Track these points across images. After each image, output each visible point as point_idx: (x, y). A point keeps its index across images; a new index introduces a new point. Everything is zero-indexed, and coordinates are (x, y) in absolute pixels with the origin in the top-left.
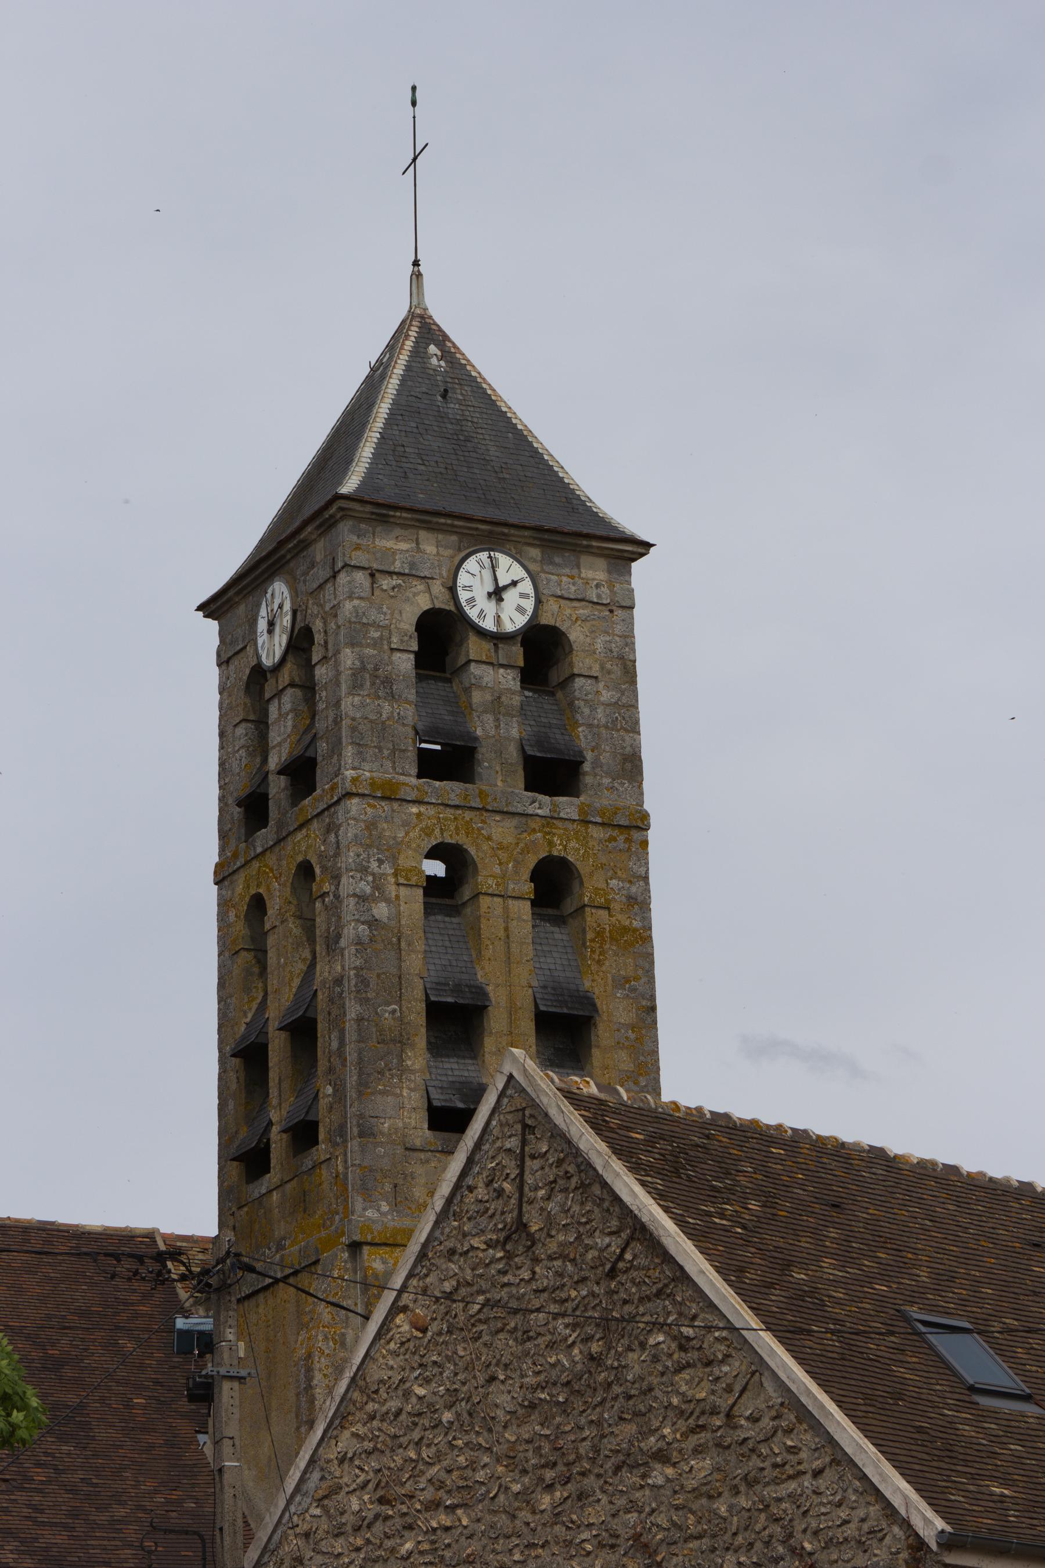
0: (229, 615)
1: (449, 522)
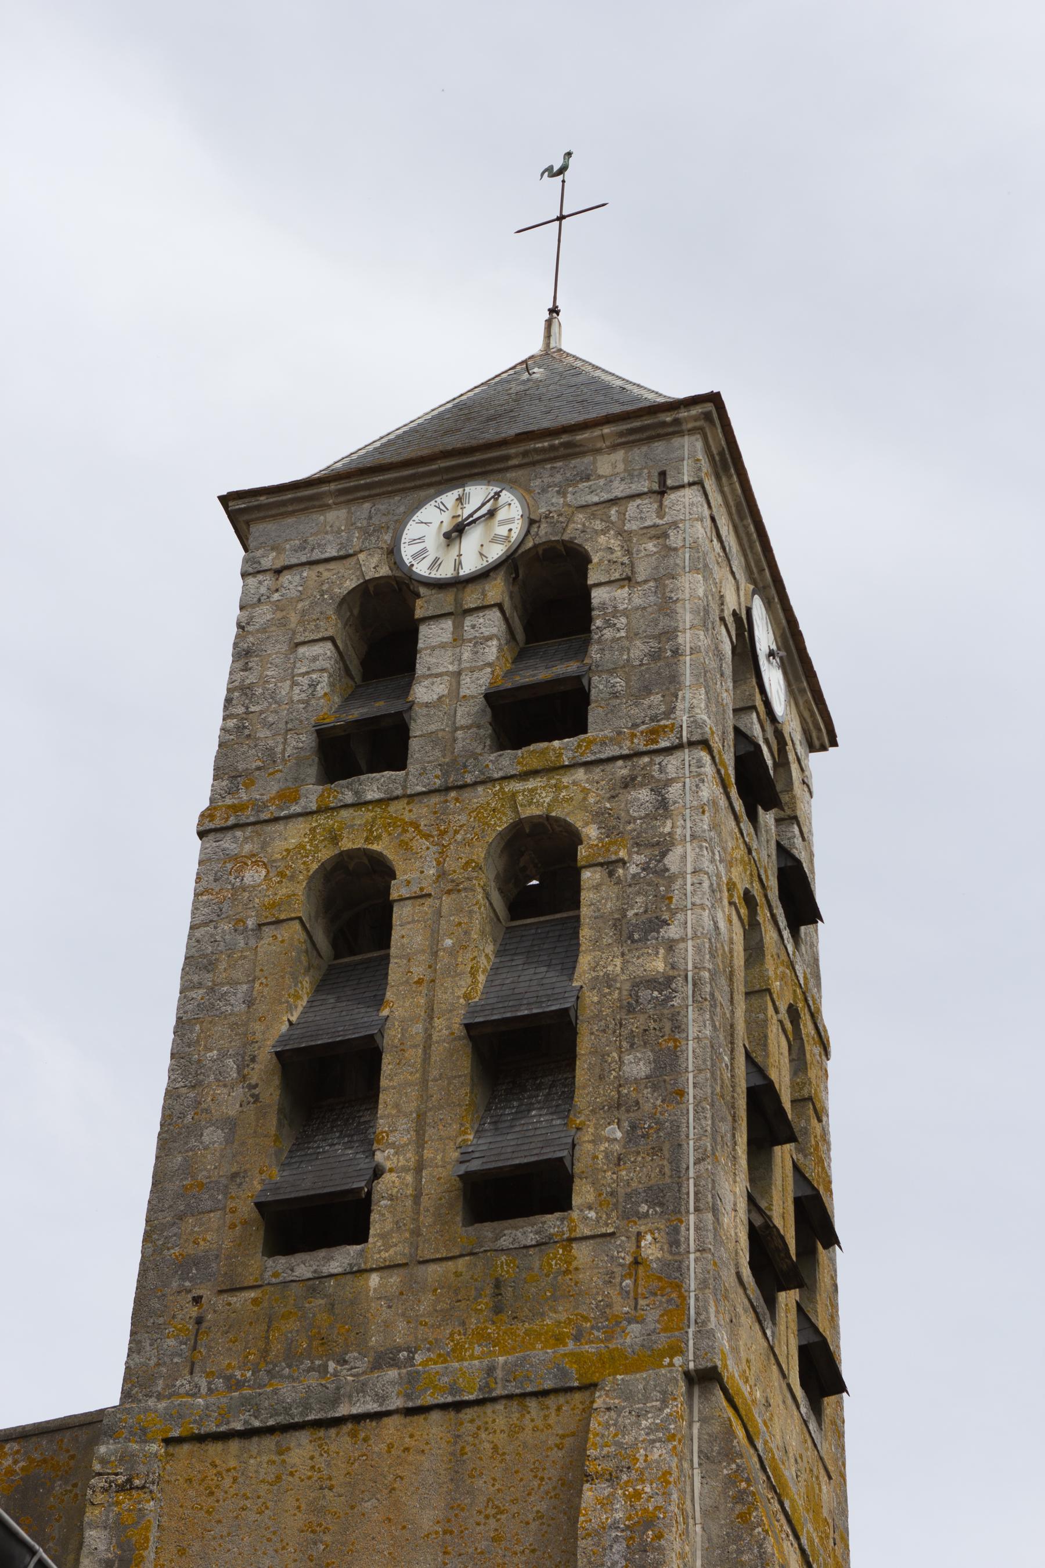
0: (290, 520)
1: (755, 536)
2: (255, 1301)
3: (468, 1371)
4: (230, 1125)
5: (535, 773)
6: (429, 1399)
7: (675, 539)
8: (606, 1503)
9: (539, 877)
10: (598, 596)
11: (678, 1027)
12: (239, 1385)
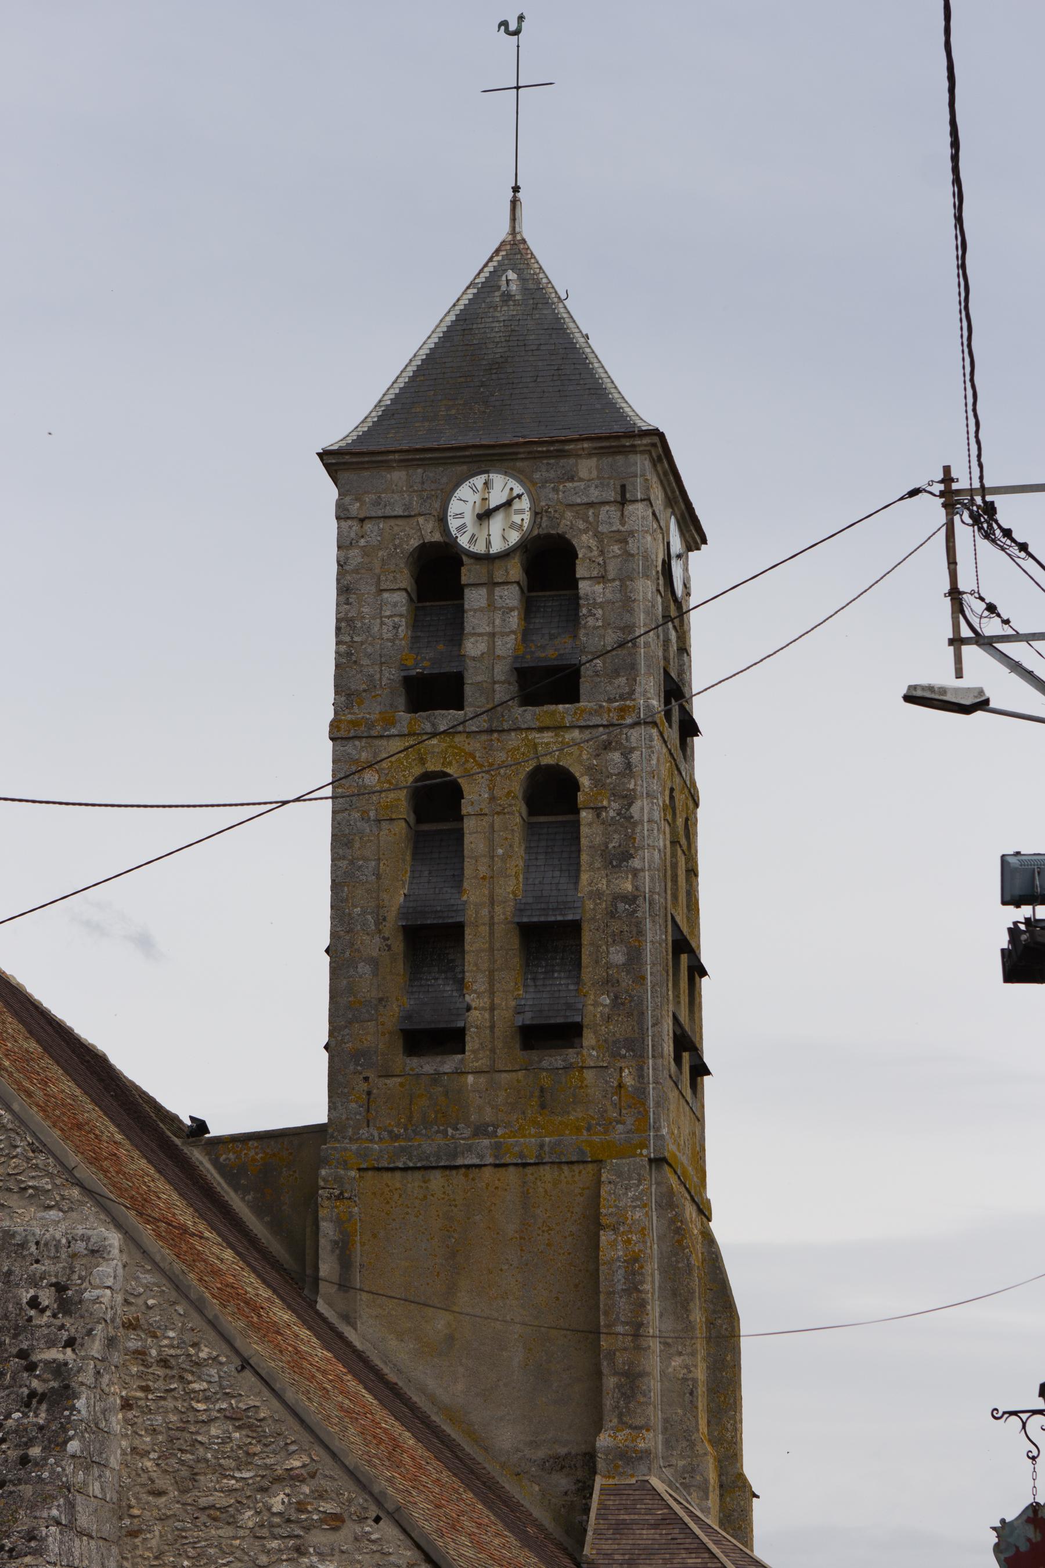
0: (366, 474)
2: (401, 1085)
3: (528, 1143)
4: (374, 963)
5: (547, 728)
6: (507, 1160)
7: (632, 547)
8: (613, 1244)
9: (552, 794)
10: (584, 587)
11: (641, 933)
12: (396, 1137)
